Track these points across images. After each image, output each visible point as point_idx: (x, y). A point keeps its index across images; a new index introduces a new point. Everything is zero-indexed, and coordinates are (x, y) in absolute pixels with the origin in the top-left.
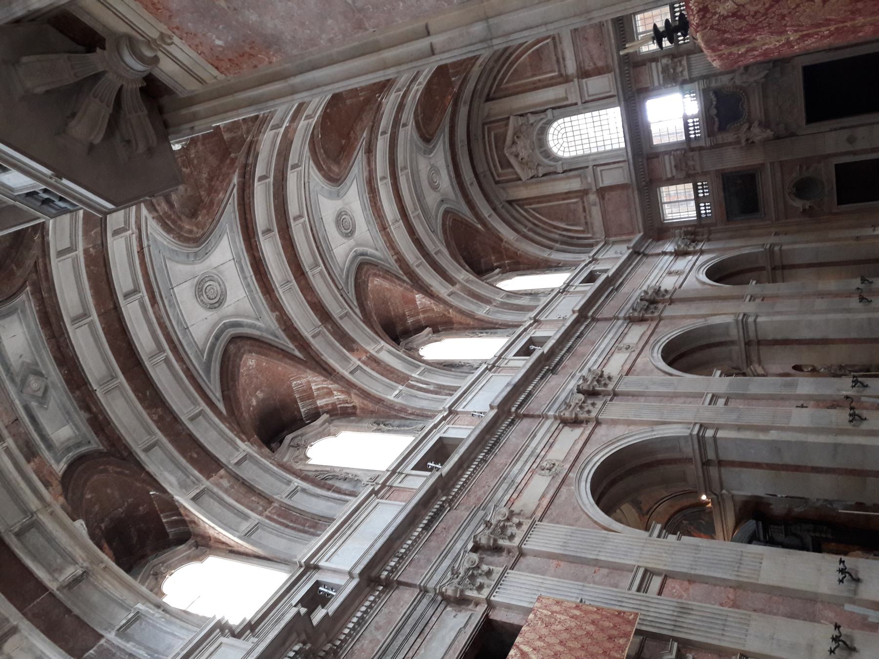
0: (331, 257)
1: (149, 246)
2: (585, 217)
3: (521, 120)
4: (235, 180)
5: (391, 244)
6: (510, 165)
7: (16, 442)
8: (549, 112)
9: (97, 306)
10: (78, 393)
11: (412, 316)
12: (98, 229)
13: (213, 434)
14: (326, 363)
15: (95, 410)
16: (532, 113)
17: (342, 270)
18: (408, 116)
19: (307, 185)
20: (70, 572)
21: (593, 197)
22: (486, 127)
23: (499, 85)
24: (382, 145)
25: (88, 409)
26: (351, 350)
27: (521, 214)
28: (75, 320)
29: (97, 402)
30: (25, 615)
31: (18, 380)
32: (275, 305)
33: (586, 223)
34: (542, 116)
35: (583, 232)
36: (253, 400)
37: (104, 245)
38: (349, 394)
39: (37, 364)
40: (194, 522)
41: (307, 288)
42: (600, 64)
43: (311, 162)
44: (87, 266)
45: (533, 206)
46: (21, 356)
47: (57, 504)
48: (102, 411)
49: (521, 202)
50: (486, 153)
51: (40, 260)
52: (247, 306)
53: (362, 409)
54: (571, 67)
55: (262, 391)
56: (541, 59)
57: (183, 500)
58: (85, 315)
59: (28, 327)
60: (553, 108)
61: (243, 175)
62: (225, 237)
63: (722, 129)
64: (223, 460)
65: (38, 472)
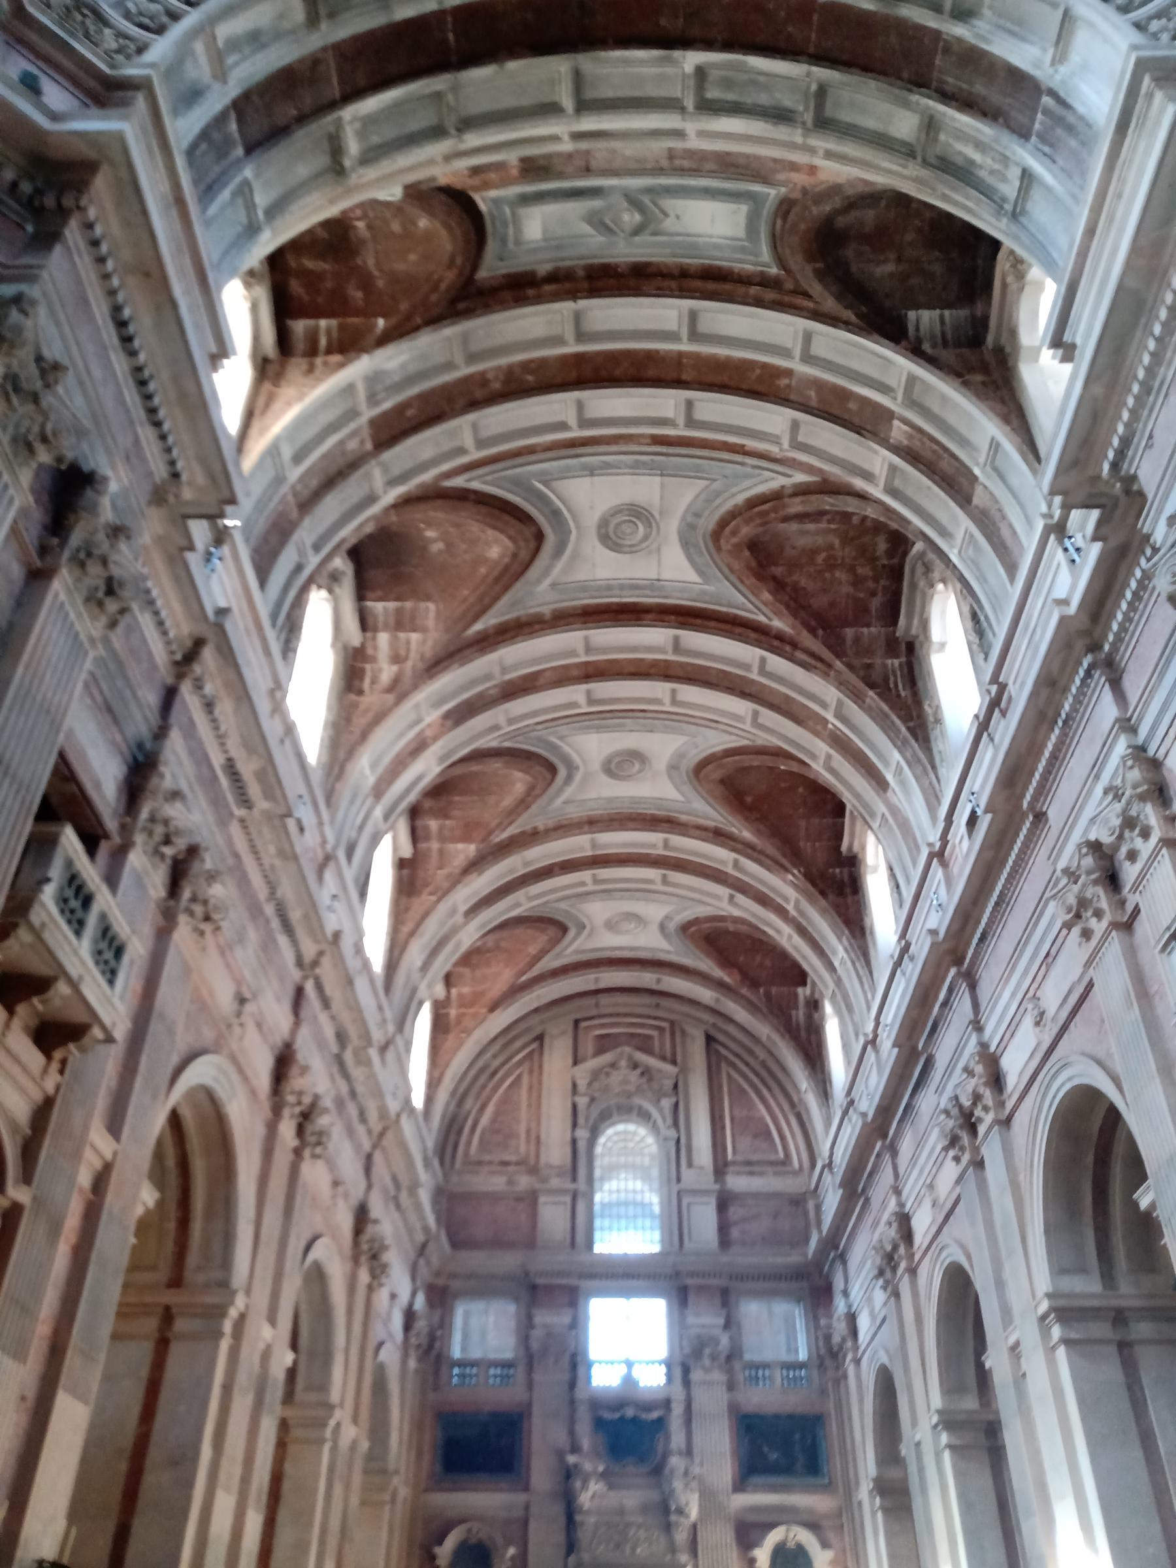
0: (588, 727)
1: (742, 464)
2: (490, 1163)
3: (668, 1084)
4: (778, 624)
5: (563, 828)
6: (600, 1051)
7: (559, 155)
8: (673, 1133)
9: (697, 356)
10: (581, 273)
11: (441, 828)
12: (814, 402)
13: (428, 453)
14: (446, 668)
15: (548, 288)
16: (676, 1105)
17: (561, 738)
18: (745, 909)
19: (714, 725)
20: (353, 147)
21: (524, 1182)
22: (665, 1025)
23: (726, 1059)
24: (721, 856)
25: (554, 277)
26: (447, 716)
27: (518, 1052)
28: (693, 316)
29: (556, 297)
30: (324, 49)
31: (646, 200)
32: (562, 619)
33: (480, 1163)
34: (669, 1121)
35: (466, 1154)
36: (434, 532)
37: (783, 400)
38: (390, 690)
39: (655, 234)
40: (311, 369)
41: (565, 677)
42: (735, 1233)
43: (750, 743)
44: (765, 366)
45: (525, 1080)
46: (678, 217)
47: (443, 174)
48: (539, 300)
49: (536, 1055)
50: (626, 1015)
51: (811, 305)
52: (581, 574)
53: (355, 706)
54: (737, 1182)
55: (440, 551)
56: (756, 1136)
57: (360, 367)
58: (694, 335)
59: (716, 247)
60: (678, 1141)
61: (780, 637)
62: (697, 579)
63: (599, 1424)
64: (387, 455)
65: (500, 166)
